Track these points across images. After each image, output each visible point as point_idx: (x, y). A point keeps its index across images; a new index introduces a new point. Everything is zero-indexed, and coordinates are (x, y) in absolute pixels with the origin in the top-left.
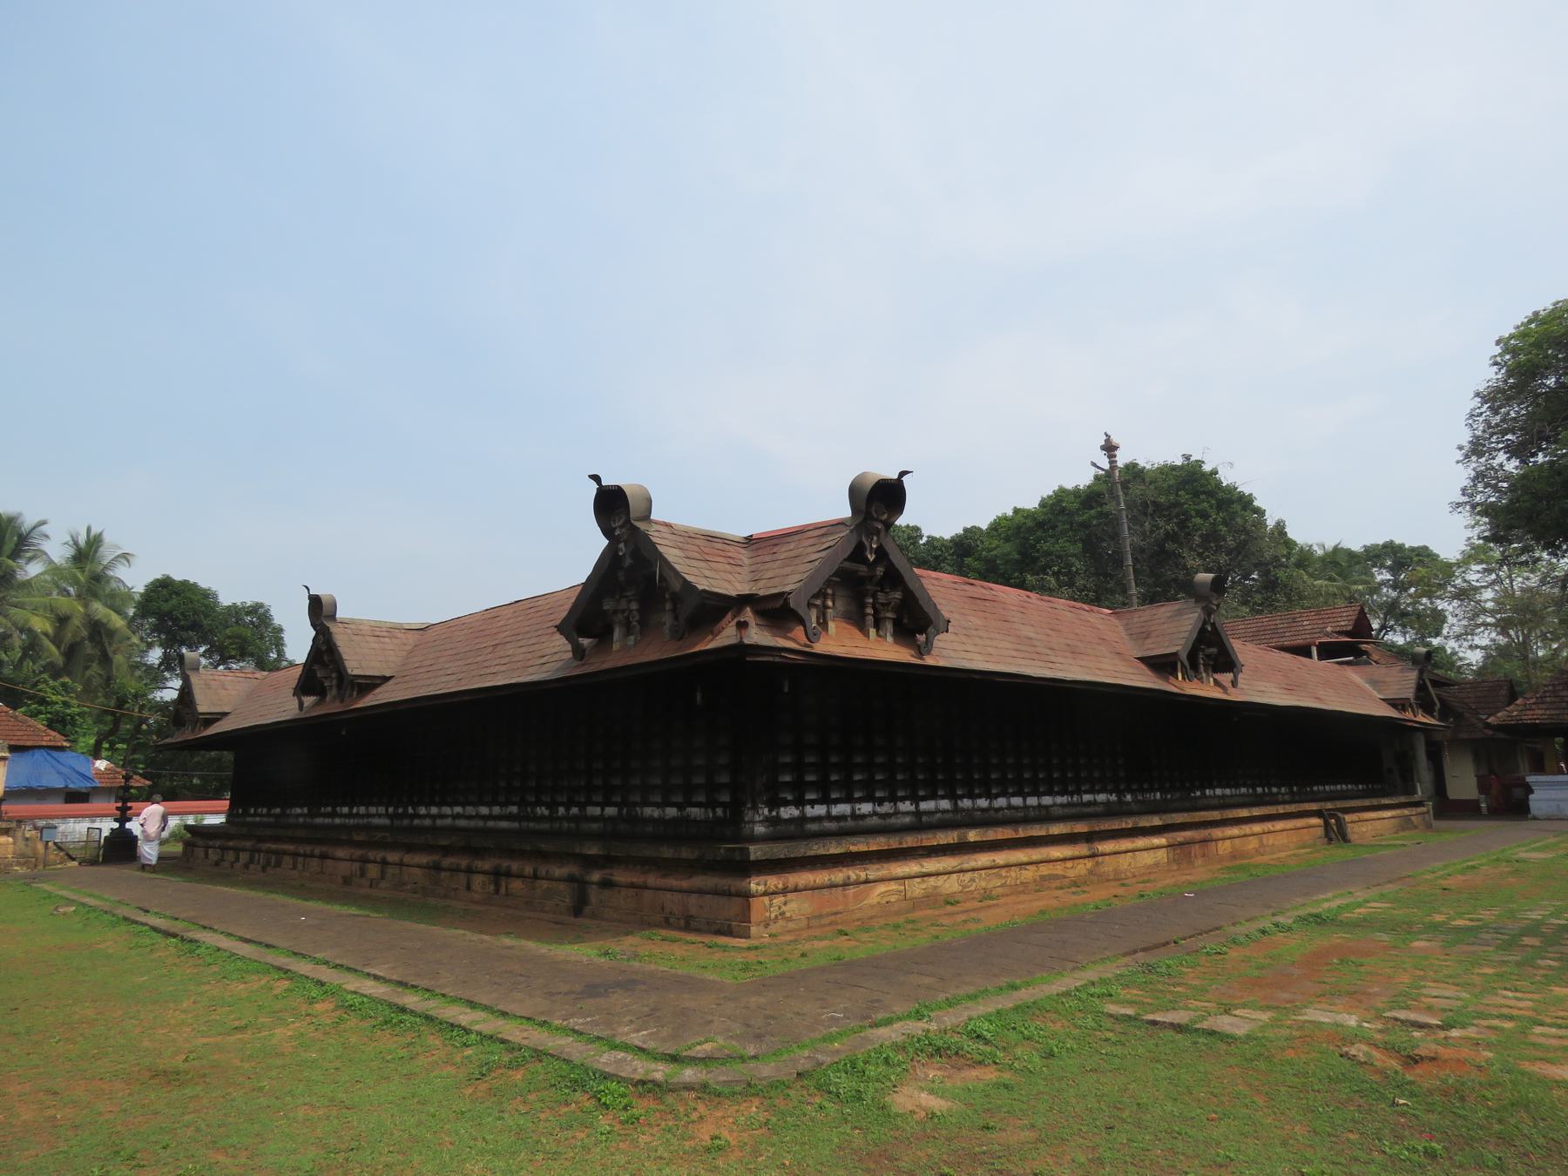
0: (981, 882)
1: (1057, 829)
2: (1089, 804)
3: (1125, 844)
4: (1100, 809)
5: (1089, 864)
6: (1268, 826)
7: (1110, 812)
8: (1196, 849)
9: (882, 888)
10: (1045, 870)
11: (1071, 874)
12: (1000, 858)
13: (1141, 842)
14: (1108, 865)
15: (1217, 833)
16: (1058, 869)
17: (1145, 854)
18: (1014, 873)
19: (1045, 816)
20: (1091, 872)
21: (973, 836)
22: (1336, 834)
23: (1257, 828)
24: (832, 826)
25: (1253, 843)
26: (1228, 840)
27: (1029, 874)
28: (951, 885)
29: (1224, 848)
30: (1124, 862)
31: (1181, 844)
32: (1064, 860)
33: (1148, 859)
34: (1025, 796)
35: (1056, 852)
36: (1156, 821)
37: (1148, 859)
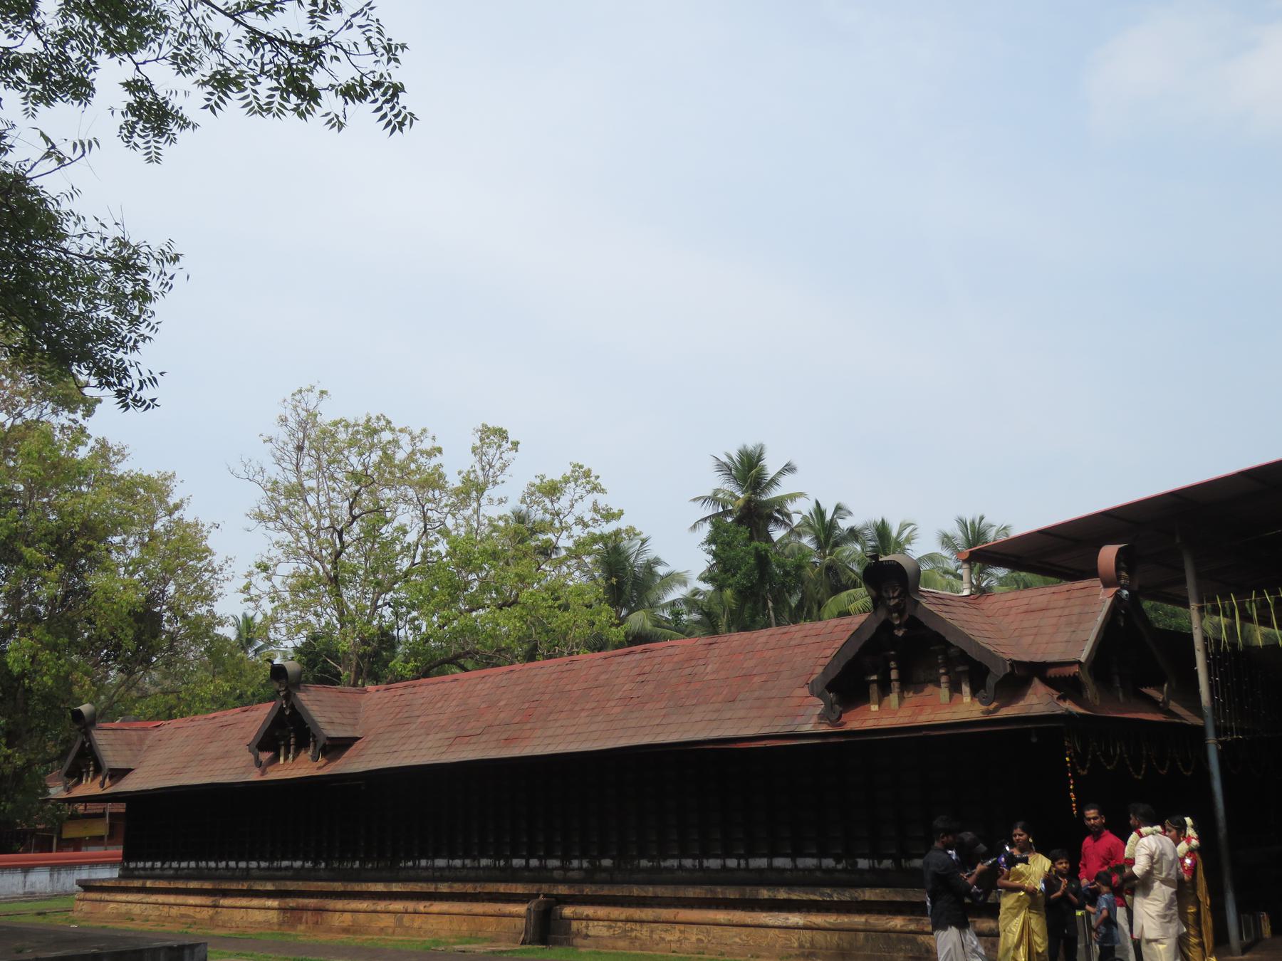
0: (152, 912)
1: (193, 885)
2: (287, 868)
3: (244, 902)
4: (290, 873)
5: (211, 911)
6: (411, 905)
7: (298, 875)
8: (307, 916)
9: (112, 905)
10: (183, 910)
11: (198, 916)
12: (161, 898)
13: (256, 902)
14: (225, 915)
15: (340, 904)
16: (191, 911)
17: (257, 912)
18: (166, 909)
19: (246, 875)
20: (211, 918)
21: (149, 884)
22: (547, 928)
23: (398, 906)
24: (142, 872)
25: (387, 921)
26: (344, 913)
27: (174, 911)
28: (136, 909)
29: (337, 920)
30: (238, 914)
31: (293, 909)
32: (196, 906)
33: (258, 916)
34: (180, 861)
35: (192, 900)
36: (269, 886)
37: (258, 916)
